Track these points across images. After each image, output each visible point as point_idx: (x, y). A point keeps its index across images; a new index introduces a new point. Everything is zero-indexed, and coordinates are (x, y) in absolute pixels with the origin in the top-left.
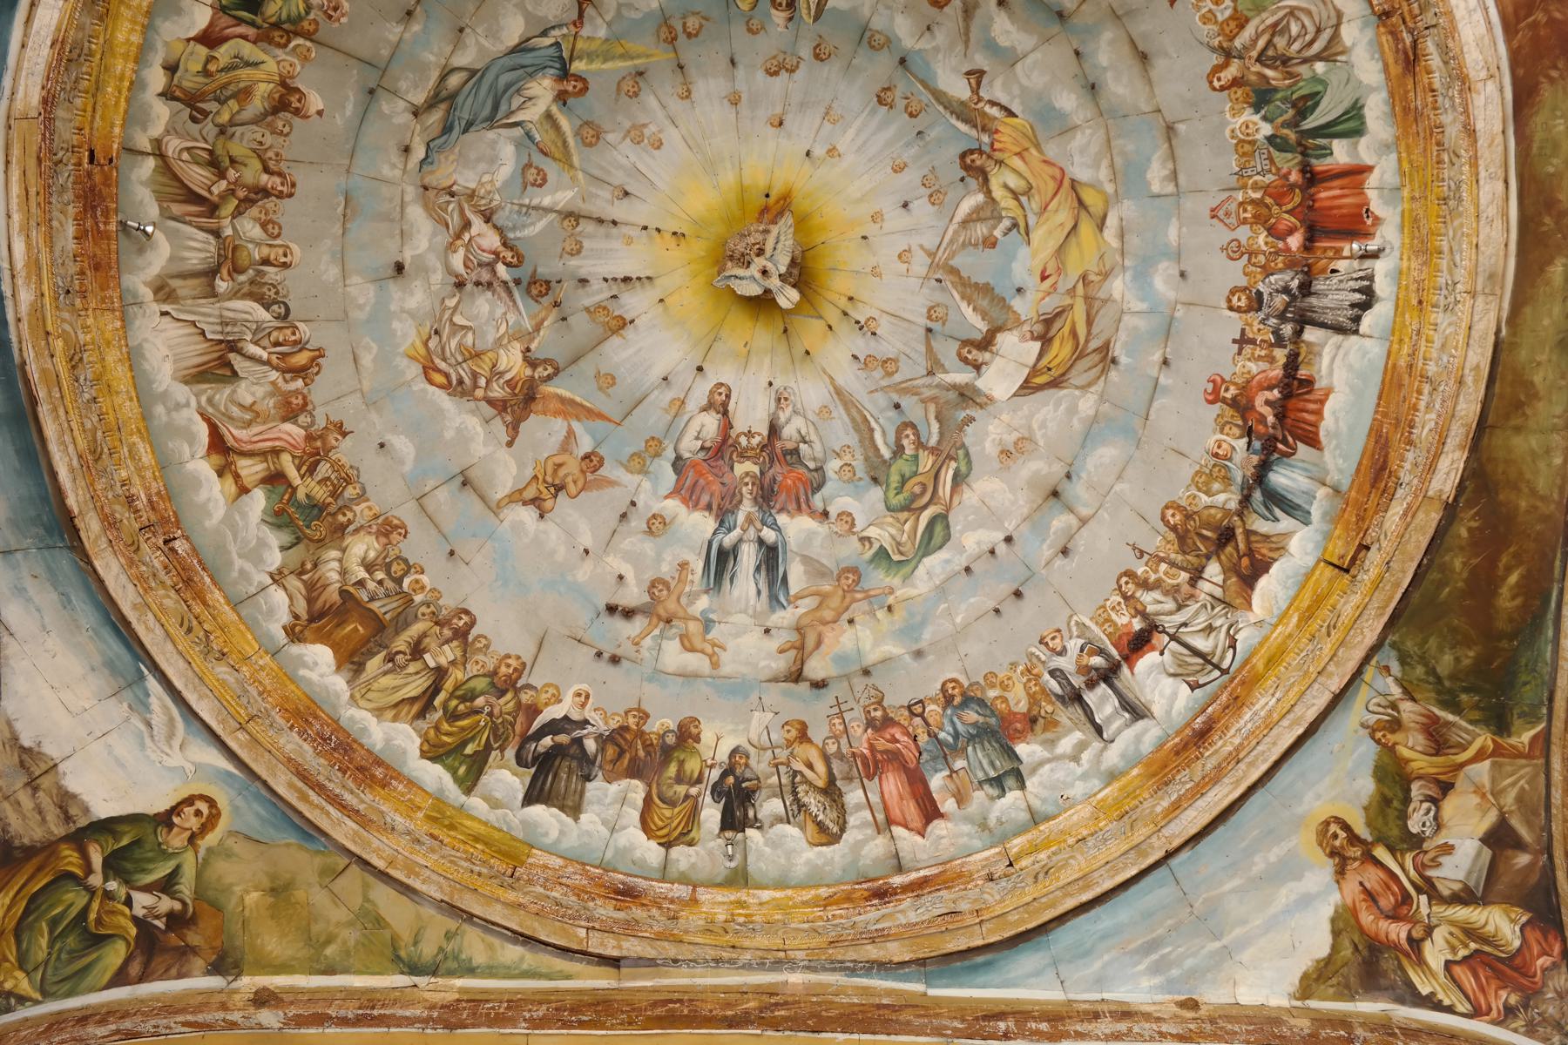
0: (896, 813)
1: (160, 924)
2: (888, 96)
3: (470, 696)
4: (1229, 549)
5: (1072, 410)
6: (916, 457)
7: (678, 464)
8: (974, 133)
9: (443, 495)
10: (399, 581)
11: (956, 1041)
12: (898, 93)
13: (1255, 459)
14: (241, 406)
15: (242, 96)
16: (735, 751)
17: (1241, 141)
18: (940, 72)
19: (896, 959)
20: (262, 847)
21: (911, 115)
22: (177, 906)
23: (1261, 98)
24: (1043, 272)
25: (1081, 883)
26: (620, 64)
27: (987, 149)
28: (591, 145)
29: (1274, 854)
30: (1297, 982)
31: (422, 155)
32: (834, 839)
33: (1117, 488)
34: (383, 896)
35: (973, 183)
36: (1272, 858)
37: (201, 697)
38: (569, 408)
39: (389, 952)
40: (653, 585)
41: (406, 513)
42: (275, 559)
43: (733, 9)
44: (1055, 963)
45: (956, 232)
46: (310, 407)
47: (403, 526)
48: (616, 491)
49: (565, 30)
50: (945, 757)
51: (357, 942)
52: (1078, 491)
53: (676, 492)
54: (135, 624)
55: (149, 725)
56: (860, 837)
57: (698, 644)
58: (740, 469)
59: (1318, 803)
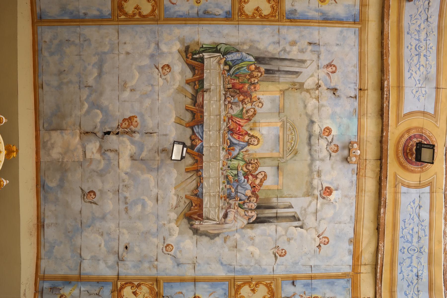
11: (443, 194)
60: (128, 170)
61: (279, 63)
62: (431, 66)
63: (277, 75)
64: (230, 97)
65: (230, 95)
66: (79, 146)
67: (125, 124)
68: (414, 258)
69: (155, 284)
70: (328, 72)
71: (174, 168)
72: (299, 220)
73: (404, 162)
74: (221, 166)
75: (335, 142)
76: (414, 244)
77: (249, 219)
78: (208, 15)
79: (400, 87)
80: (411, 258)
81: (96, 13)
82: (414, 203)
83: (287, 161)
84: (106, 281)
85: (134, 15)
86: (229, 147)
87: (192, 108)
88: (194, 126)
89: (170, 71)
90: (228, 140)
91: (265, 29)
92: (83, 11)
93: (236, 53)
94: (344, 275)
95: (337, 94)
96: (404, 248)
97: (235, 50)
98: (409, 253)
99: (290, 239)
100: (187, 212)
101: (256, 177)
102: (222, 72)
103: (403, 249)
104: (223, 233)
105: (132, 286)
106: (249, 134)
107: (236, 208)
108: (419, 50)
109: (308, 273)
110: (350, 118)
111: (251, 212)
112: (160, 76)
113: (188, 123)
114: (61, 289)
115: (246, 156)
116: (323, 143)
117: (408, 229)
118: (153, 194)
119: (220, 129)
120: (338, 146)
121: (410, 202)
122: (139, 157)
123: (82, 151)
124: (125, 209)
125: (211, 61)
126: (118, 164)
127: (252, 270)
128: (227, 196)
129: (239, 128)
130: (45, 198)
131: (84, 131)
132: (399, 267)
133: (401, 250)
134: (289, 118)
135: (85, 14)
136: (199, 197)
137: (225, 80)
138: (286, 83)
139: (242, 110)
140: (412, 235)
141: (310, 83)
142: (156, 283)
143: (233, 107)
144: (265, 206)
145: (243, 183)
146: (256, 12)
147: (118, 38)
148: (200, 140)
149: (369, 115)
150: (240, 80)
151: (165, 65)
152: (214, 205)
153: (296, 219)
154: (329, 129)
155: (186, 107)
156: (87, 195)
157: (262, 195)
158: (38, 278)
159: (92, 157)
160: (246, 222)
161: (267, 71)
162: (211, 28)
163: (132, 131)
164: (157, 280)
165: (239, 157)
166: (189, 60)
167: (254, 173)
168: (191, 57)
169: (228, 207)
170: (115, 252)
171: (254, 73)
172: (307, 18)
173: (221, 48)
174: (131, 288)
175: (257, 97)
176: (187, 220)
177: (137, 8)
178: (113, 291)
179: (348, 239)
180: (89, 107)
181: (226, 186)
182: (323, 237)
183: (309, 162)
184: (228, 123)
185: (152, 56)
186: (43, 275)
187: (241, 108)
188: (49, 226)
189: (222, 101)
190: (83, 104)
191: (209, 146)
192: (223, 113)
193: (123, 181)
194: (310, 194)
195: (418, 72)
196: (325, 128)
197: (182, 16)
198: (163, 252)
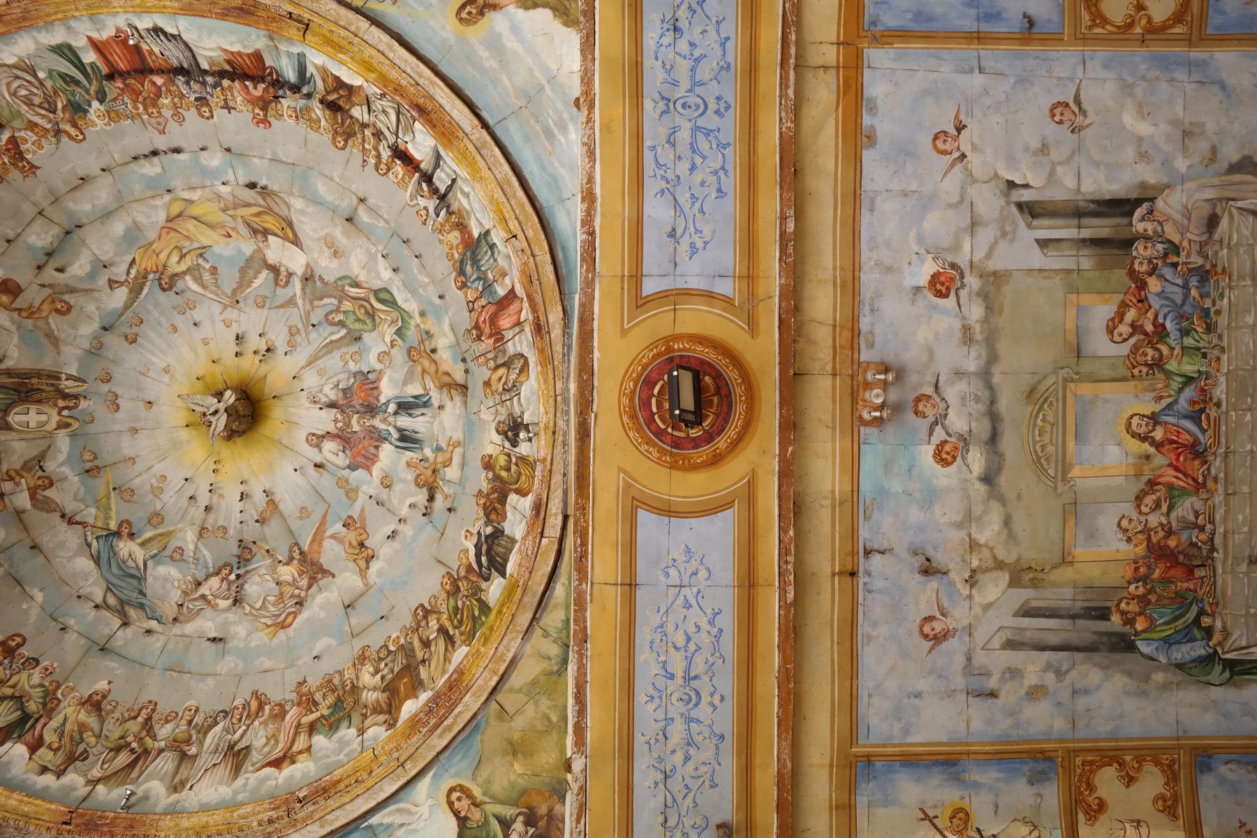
0: (512, 320)
1: (531, 831)
2: (131, 337)
3: (456, 608)
4: (341, 103)
5: (303, 212)
6: (345, 312)
7: (352, 467)
8: (148, 284)
9: (354, 621)
10: (390, 652)
11: (597, 270)
12: (128, 331)
13: (288, 93)
14: (266, 745)
15: (83, 729)
16: (498, 432)
17: (109, 118)
18: (112, 306)
19: (561, 316)
20: (484, 759)
21: (142, 322)
22: (521, 818)
23: (78, 109)
24: (224, 236)
25: (505, 187)
26: (113, 500)
27: (157, 275)
28: (163, 519)
29: (483, 53)
30: (569, 29)
31: (155, 622)
32: (526, 359)
33: (337, 180)
34: (518, 679)
35: (180, 285)
36: (486, 54)
37: (382, 790)
38: (318, 538)
39: (554, 678)
40: (418, 485)
41: (358, 644)
42: (353, 731)
43: (78, 432)
44: (562, 201)
45: (211, 292)
46: (283, 702)
47: (364, 648)
48: (366, 508)
49: (89, 533)
50: (489, 286)
51: (548, 699)
52: (347, 203)
53: (368, 469)
54: (333, 828)
55: (402, 825)
56: (525, 343)
57: (448, 455)
58: (356, 428)
59: (448, 27)
61: (1074, 638)
62: (651, 647)
63: (1080, 604)
65: (1200, 548)
68: (685, 84)
70: (944, 619)
72: (1020, 206)
73: (728, 367)
74: (1225, 358)
75: (923, 424)
76: (689, 125)
77: (1151, 212)
79: (749, 583)
80: (695, 83)
82: (692, 245)
83: (1055, 372)
86: (1203, 410)
91: (1109, 728)
94: (885, 39)
95: (921, 559)
96: (717, 112)
98: (702, 99)
99: (1042, 151)
101: (1136, 328)
102: (1218, 610)
103: (722, 109)
104: (1220, 175)
106: (1151, 444)
107: (1185, 244)
108: (690, 693)
109: (989, 52)
110: (882, 492)
111: (1145, 230)
115: (1160, 386)
116: (957, 422)
117: (708, 170)
120: (916, 413)
121: (704, 248)
127: (1143, 67)
129: (1177, 459)
132: (730, 57)
133: (727, 108)
134: (1050, 490)
138: (1054, 585)
139: (1170, 509)
140: (694, 152)
141: (994, 587)
143: (1192, 518)
145: (1169, 312)
146: (1133, 774)
149: (827, 503)
153: (1027, 207)
154: (942, 460)
157: (1120, 276)
160: (1160, 204)
161: (1103, 614)
167: (1139, 340)
171: (1137, 609)
172: (1000, 764)
179: (878, 146)
181: (1214, 303)
182: (951, 153)
183: (996, 369)
187: (1173, 515)
192: (1218, 499)
194: (992, 279)
195: (692, 629)
196: (951, 463)
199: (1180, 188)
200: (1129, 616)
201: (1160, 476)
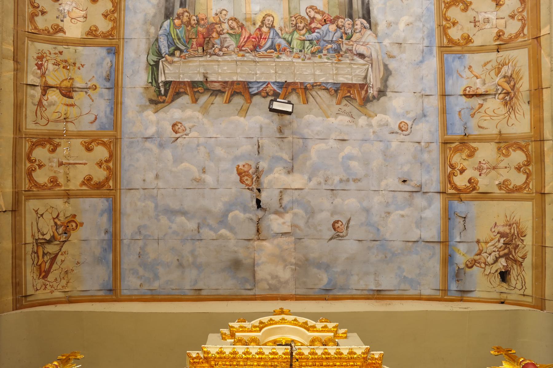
60: (306, 177)
64: (214, 49)
65: (212, 49)
66: (276, 241)
67: (247, 180)
69: (449, 146)
71: (303, 118)
74: (300, 60)
77: (365, 28)
78: (111, 76)
81: (105, 218)
84: (447, 208)
85: (108, 168)
86: (276, 50)
87: (227, 96)
88: (250, 93)
89: (181, 123)
90: (268, 51)
91: (130, 6)
92: (103, 234)
93: (159, 42)
97: (156, 43)
100: (358, 103)
101: (313, 19)
102: (182, 59)
104: (383, 60)
105: (453, 174)
107: (351, 43)
111: (357, 25)
112: (186, 135)
113: (246, 100)
114: (459, 268)
115: (287, 30)
118: (336, 146)
119: (253, 61)
122: (289, 162)
123: (281, 237)
124: (355, 183)
125: (169, 72)
126: (298, 191)
127: (428, 26)
128: (337, 54)
129: (253, 38)
130: (342, 289)
131: (256, 235)
135: (106, 232)
136: (338, 88)
137: (192, 55)
142: (448, 145)
143: (226, 45)
144: (348, 9)
145: (320, 34)
147: (138, 189)
148: (267, 85)
150: (194, 37)
151: (172, 129)
152: (348, 69)
155: (226, 103)
156: (338, 232)
157: (335, 12)
158: (445, 297)
159: (290, 224)
160: (369, 32)
162: (128, 71)
163: (256, 172)
164: (444, 143)
165: (288, 38)
166: (167, 99)
167: (307, 21)
168: (164, 97)
169: (351, 52)
170: (410, 196)
173: (153, 60)
174: (456, 176)
175: (214, 16)
176: (369, 103)
177: (100, 165)
178: (460, 200)
180: (224, 228)
181: (325, 55)
184: (247, 51)
185: (161, 146)
186: (441, 291)
187: (227, 36)
188: (378, 283)
189: (219, 58)
190: (221, 236)
191: (274, 75)
192: (234, 57)
193: (320, 184)
197: (112, 108)
198: (409, 134)
199: (376, 41)
200: (181, 17)
201: (245, 30)
